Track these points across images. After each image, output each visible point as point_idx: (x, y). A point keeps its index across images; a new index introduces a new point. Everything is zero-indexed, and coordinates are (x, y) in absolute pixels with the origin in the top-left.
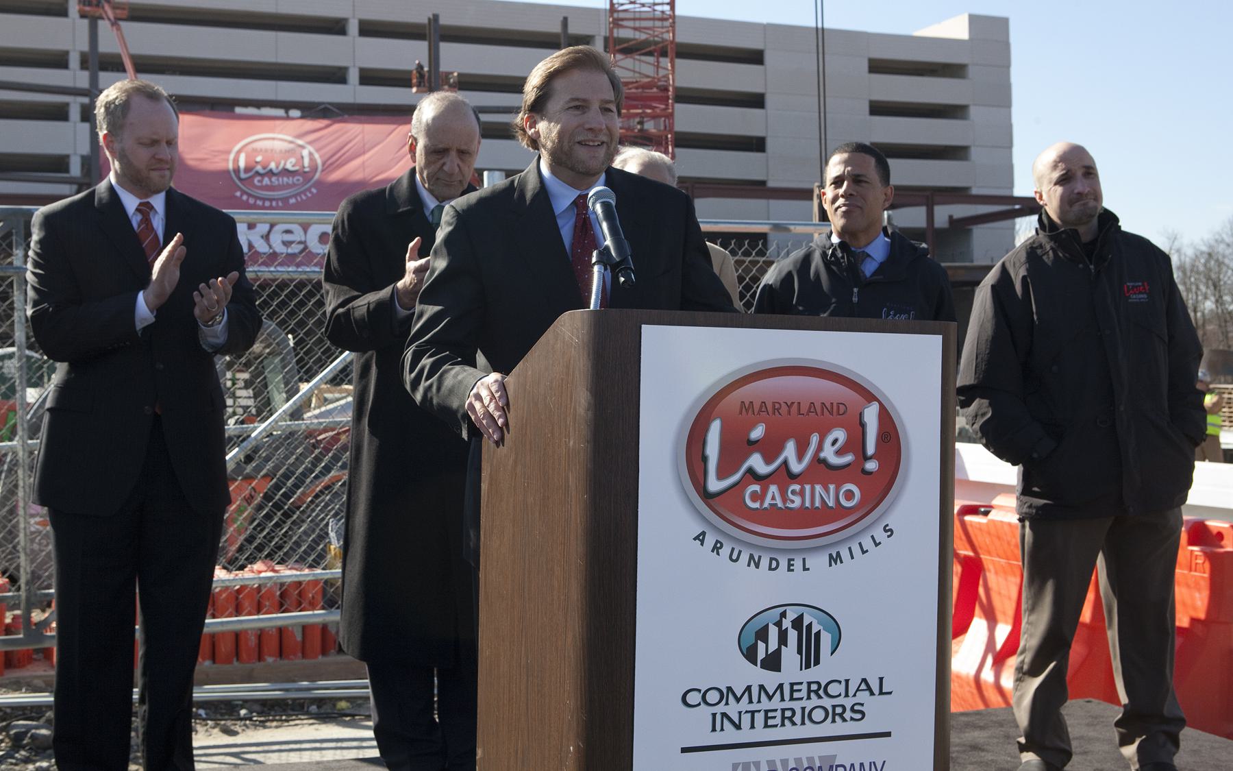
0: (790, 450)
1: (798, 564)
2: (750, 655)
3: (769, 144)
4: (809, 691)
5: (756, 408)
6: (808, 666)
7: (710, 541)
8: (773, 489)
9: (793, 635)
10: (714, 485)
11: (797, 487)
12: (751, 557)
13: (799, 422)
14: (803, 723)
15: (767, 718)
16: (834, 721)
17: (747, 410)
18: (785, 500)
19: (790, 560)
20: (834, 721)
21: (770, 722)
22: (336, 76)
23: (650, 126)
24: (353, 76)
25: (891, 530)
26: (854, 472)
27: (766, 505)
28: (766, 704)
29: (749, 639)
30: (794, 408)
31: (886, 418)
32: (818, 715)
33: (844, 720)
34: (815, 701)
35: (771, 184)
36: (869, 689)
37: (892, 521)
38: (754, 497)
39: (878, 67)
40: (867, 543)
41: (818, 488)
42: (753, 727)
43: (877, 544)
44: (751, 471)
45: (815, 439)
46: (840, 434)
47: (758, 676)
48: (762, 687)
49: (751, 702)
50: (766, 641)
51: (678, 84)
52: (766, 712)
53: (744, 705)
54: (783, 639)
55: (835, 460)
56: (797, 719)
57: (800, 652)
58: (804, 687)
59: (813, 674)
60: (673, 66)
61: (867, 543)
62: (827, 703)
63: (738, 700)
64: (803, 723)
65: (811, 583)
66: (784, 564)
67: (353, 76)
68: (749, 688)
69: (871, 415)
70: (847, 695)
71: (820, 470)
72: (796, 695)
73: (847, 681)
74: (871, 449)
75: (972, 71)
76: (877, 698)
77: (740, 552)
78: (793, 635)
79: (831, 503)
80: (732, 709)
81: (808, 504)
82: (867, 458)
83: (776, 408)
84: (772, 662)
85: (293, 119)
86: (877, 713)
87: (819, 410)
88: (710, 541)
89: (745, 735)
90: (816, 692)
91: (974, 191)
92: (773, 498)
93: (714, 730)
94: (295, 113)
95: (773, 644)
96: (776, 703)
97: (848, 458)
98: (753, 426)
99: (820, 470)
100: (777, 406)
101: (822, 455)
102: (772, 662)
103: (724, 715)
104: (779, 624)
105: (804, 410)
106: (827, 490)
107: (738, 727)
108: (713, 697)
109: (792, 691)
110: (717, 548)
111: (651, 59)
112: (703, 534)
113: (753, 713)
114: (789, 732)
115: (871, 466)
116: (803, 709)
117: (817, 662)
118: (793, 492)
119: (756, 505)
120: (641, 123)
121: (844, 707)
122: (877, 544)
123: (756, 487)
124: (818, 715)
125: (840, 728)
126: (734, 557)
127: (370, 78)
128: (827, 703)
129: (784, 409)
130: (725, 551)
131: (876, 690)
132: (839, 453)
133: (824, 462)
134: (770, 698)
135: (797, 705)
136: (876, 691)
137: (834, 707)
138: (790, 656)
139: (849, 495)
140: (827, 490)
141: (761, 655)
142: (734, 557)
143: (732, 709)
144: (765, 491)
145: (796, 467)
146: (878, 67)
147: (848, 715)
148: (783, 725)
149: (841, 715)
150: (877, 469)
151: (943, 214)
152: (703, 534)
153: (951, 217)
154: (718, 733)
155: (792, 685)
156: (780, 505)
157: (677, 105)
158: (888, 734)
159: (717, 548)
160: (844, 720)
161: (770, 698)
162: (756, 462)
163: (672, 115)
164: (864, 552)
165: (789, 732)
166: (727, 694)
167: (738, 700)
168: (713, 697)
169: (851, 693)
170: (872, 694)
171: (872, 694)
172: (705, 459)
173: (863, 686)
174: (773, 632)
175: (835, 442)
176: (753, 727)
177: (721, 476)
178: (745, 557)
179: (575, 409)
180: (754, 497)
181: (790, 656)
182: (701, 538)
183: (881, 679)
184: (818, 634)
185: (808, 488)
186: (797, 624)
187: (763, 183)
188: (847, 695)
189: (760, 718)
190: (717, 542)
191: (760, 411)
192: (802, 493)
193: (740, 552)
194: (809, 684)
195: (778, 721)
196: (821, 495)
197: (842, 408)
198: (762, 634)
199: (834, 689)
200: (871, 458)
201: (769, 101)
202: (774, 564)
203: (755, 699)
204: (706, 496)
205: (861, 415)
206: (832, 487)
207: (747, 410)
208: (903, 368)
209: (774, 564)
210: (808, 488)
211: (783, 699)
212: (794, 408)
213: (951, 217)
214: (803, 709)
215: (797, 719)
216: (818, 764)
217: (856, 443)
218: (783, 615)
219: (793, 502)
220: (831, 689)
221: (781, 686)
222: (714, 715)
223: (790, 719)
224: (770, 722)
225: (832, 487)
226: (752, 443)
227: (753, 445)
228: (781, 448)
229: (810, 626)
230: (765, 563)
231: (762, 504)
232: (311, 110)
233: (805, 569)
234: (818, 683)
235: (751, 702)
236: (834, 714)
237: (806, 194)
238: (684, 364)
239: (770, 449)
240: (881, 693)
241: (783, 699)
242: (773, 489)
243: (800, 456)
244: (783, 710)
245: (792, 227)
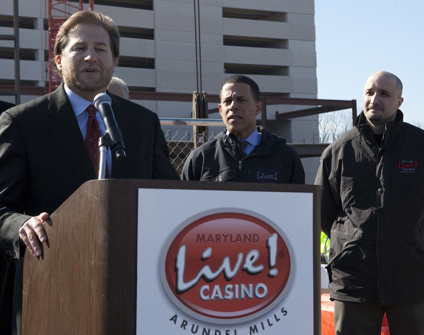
0: (226, 264)
3: (157, 63)
5: (206, 237)
7: (180, 320)
8: (217, 288)
10: (182, 286)
11: (230, 286)
12: (204, 330)
13: (230, 246)
17: (201, 240)
18: (223, 294)
19: (227, 331)
25: (286, 311)
27: (213, 297)
30: (228, 238)
31: (281, 242)
35: (158, 90)
37: (286, 305)
38: (206, 293)
39: (229, 13)
40: (272, 320)
41: (243, 286)
43: (278, 320)
44: (203, 277)
45: (240, 256)
46: (255, 253)
55: (252, 269)
61: (272, 320)
69: (273, 241)
71: (245, 276)
74: (273, 262)
75: (289, 17)
77: (198, 327)
79: (251, 296)
81: (237, 296)
82: (271, 268)
83: (218, 238)
88: (180, 320)
91: (292, 96)
92: (217, 293)
98: (204, 250)
99: (245, 276)
100: (218, 237)
101: (245, 266)
105: (234, 238)
106: (248, 287)
110: (184, 325)
112: (176, 316)
115: (274, 272)
118: (229, 289)
119: (206, 298)
122: (278, 320)
123: (207, 287)
126: (194, 330)
129: (223, 238)
130: (189, 327)
132: (255, 265)
133: (246, 270)
139: (261, 290)
140: (248, 287)
142: (194, 330)
144: (212, 289)
145: (230, 274)
146: (229, 13)
150: (277, 275)
151: (272, 111)
152: (176, 316)
153: (277, 113)
156: (221, 297)
159: (184, 325)
162: (207, 271)
164: (270, 325)
172: (176, 270)
175: (252, 258)
177: (186, 280)
179: (95, 241)
180: (206, 293)
182: (174, 319)
185: (237, 286)
187: (153, 89)
190: (184, 321)
192: (233, 290)
193: (198, 327)
196: (245, 290)
197: (256, 238)
200: (273, 267)
201: (157, 34)
204: (177, 293)
205: (267, 242)
206: (251, 286)
207: (201, 240)
208: (290, 212)
212: (228, 238)
213: (277, 113)
217: (264, 259)
219: (228, 295)
225: (251, 286)
227: (204, 261)
228: (221, 262)
231: (210, 297)
237: (188, 97)
238: (162, 212)
239: (214, 263)
242: (217, 288)
243: (232, 267)
245: (188, 122)
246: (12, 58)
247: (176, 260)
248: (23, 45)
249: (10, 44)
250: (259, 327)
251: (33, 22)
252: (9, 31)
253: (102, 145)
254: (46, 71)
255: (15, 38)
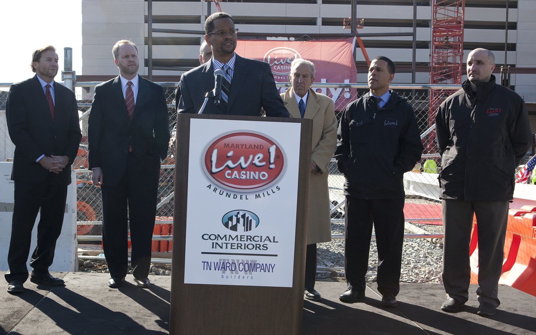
0: (242, 160)
1: (244, 197)
2: (226, 225)
4: (247, 239)
6: (247, 230)
7: (213, 187)
8: (236, 172)
9: (241, 220)
10: (214, 170)
11: (244, 172)
12: (227, 194)
14: (245, 249)
15: (232, 246)
16: (256, 249)
18: (240, 176)
20: (256, 249)
21: (233, 247)
22: (312, 22)
23: (451, 40)
24: (319, 22)
26: (266, 168)
27: (233, 177)
28: (231, 241)
29: (226, 220)
30: (244, 146)
31: (278, 150)
32: (250, 247)
33: (260, 249)
34: (249, 242)
36: (269, 240)
38: (229, 174)
40: (270, 192)
41: (252, 173)
42: (227, 248)
43: (273, 193)
44: (227, 166)
45: (251, 157)
47: (229, 232)
48: (230, 236)
49: (226, 240)
50: (232, 221)
51: (465, 20)
52: (232, 244)
53: (224, 241)
54: (238, 221)
56: (243, 247)
57: (244, 225)
58: (245, 237)
59: (249, 233)
60: (464, 12)
61: (270, 192)
62: (254, 243)
63: (222, 239)
64: (245, 249)
65: (250, 203)
66: (239, 197)
67: (319, 22)
68: (225, 236)
69: (273, 150)
70: (261, 241)
71: (253, 167)
72: (242, 239)
73: (261, 237)
74: (272, 161)
76: (272, 243)
78: (241, 220)
80: (220, 242)
81: (248, 178)
82: (270, 164)
83: (237, 146)
84: (234, 228)
85: (291, 41)
86: (272, 248)
87: (253, 147)
88: (213, 187)
89: (224, 250)
90: (250, 239)
93: (213, 247)
94: (292, 39)
95: (234, 222)
96: (235, 241)
97: (264, 163)
98: (229, 152)
99: (253, 167)
101: (254, 162)
102: (234, 228)
103: (216, 243)
104: (237, 216)
105: (247, 147)
106: (255, 174)
107: (222, 248)
108: (213, 237)
109: (241, 238)
110: (215, 190)
111: (453, 8)
112: (210, 185)
113: (227, 244)
114: (239, 251)
115: (272, 166)
116: (245, 244)
117: (250, 229)
118: (243, 174)
119: (229, 177)
120: (447, 39)
121: (260, 245)
122: (273, 193)
123: (230, 172)
124: (250, 247)
125: (258, 252)
127: (326, 22)
128: (254, 243)
129: (240, 146)
130: (218, 191)
131: (272, 240)
132: (260, 161)
133: (255, 164)
134: (233, 239)
135: (243, 243)
136: (272, 241)
137: (256, 245)
138: (240, 227)
139: (264, 176)
140: (255, 174)
141: (230, 225)
143: (220, 242)
144: (232, 173)
145: (244, 166)
147: (261, 248)
148: (237, 248)
149: (259, 248)
150: (275, 168)
152: (210, 185)
154: (214, 249)
155: (241, 236)
157: (465, 29)
158: (276, 256)
159: (215, 190)
160: (260, 249)
161: (233, 239)
162: (230, 163)
163: (463, 34)
165: (239, 251)
166: (218, 237)
167: (222, 239)
168: (213, 237)
169: (263, 240)
170: (271, 242)
171: (271, 242)
172: (211, 162)
173: (267, 239)
174: (235, 219)
175: (259, 158)
176: (227, 248)
177: (217, 167)
178: (225, 194)
180: (229, 174)
181: (240, 227)
182: (209, 187)
183: (274, 237)
184: (251, 220)
185: (248, 172)
186: (243, 216)
188: (261, 241)
189: (229, 246)
191: (231, 146)
192: (246, 174)
194: (247, 236)
195: (236, 247)
196: (253, 175)
197: (262, 147)
198: (231, 219)
199: (256, 239)
201: (519, 26)
202: (235, 197)
203: (228, 239)
204: (212, 173)
206: (257, 173)
209: (235, 197)
210: (248, 172)
211: (237, 240)
212: (244, 146)
214: (245, 244)
215: (243, 247)
216: (250, 262)
217: (267, 158)
218: (238, 213)
220: (255, 239)
221: (237, 236)
222: (213, 243)
223: (240, 247)
224: (233, 247)
225: (257, 173)
226: (228, 157)
227: (228, 158)
228: (239, 159)
229: (248, 218)
230: (232, 196)
231: (231, 176)
232: (300, 37)
233: (246, 199)
234: (251, 237)
235: (226, 240)
236: (256, 247)
239: (235, 159)
240: (274, 242)
241: (237, 240)
242: (236, 172)
243: (246, 162)
244: (238, 244)
246: (411, 48)
247: (211, 156)
248: (418, 39)
249: (410, 38)
250: (261, 195)
251: (428, 23)
252: (410, 30)
253: (207, 97)
254: (430, 56)
255: (413, 34)
